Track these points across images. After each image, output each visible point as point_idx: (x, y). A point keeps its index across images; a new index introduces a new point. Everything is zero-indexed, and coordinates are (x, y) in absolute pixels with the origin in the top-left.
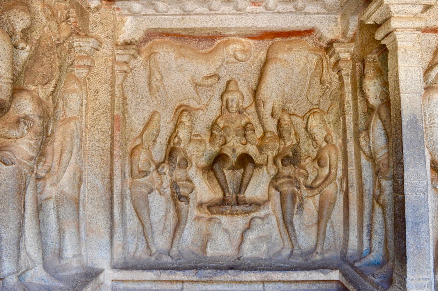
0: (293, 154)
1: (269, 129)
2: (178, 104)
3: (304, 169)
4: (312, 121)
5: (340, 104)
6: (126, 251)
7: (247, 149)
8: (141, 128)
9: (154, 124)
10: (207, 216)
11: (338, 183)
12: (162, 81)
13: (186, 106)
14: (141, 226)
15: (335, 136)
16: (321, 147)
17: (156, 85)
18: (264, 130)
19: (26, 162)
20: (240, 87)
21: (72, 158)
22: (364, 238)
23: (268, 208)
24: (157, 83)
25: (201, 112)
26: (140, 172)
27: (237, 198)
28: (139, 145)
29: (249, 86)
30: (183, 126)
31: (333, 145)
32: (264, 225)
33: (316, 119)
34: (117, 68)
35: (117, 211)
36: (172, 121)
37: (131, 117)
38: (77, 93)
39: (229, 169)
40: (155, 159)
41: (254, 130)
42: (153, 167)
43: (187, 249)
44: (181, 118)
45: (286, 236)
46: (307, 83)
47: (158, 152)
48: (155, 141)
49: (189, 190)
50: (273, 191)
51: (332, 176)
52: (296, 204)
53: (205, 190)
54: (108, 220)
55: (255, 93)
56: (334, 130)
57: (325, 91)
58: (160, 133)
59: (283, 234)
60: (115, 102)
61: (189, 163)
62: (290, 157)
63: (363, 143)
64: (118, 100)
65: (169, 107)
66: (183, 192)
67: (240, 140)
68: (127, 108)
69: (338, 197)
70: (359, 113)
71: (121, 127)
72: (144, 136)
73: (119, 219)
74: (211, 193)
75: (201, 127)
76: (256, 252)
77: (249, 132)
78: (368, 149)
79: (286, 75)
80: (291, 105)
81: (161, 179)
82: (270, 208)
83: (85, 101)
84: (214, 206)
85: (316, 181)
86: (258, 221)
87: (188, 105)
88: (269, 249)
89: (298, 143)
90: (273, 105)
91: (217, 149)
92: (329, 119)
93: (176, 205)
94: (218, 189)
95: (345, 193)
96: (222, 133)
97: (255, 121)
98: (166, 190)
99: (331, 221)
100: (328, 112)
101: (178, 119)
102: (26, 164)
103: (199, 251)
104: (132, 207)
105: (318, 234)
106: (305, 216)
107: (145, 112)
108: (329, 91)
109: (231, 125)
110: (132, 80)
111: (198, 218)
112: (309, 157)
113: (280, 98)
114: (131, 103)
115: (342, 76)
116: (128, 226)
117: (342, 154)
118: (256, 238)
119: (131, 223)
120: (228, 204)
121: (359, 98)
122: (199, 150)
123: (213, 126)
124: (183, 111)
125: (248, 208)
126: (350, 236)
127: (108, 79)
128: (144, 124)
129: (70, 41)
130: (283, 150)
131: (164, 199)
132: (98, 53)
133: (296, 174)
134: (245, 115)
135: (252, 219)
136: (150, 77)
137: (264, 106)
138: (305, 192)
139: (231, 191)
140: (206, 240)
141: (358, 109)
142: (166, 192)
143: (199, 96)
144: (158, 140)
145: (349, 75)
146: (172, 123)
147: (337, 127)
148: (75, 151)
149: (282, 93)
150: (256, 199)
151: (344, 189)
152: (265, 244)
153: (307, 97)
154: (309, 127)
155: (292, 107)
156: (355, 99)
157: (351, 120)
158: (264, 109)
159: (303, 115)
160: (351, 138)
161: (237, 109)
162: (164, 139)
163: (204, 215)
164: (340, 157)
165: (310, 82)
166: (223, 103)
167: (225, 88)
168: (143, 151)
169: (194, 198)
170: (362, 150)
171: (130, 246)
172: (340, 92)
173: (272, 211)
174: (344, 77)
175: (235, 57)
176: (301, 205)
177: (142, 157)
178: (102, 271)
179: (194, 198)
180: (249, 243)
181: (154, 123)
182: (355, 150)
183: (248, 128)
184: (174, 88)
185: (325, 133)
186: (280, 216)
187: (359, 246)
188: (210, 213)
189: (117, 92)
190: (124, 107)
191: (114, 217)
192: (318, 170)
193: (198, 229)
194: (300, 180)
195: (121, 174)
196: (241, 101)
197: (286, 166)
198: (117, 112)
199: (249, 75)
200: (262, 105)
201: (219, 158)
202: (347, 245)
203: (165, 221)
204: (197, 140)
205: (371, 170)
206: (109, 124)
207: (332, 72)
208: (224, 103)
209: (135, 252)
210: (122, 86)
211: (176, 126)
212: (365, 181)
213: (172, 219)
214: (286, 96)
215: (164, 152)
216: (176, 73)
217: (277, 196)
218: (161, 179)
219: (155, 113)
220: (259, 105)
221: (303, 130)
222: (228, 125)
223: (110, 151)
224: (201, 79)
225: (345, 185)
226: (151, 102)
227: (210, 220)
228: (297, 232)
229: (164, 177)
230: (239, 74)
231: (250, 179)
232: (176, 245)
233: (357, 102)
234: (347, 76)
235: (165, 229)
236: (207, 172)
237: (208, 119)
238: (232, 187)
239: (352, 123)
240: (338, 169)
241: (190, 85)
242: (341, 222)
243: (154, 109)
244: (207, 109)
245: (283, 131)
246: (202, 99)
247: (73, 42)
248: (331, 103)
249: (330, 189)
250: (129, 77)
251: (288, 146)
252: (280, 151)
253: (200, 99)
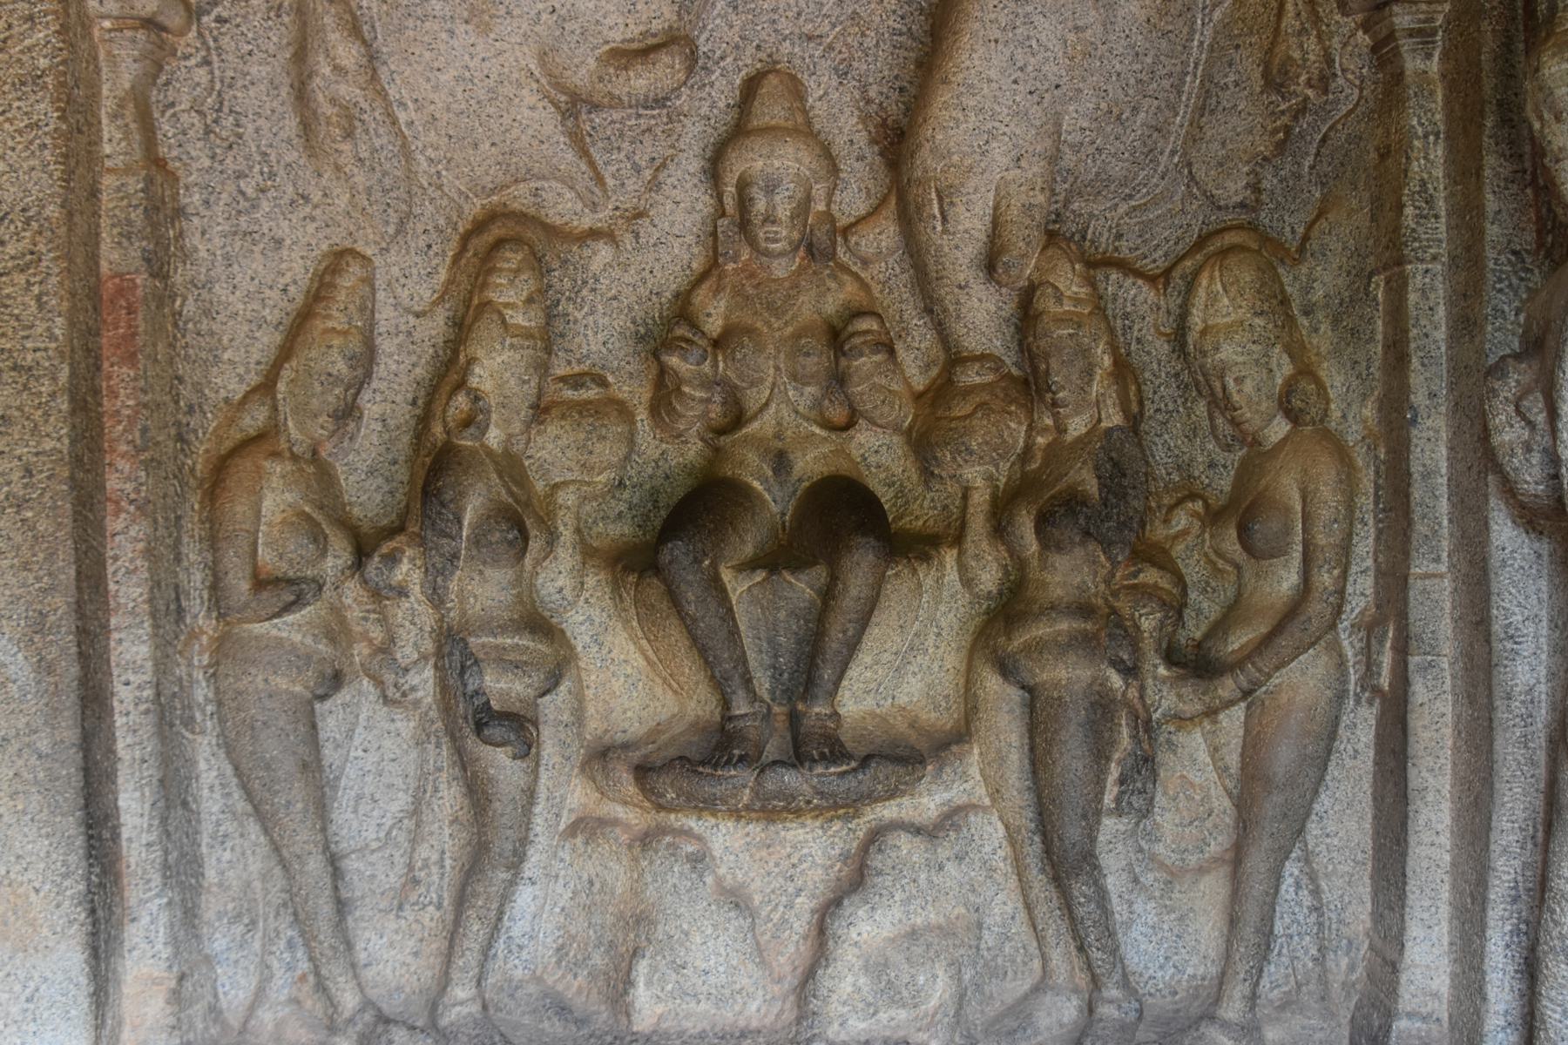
0: (1102, 486)
1: (972, 343)
2: (475, 207)
3: (1161, 568)
4: (1213, 299)
5: (1377, 204)
6: (199, 1009)
7: (856, 454)
8: (269, 339)
9: (338, 321)
10: (632, 815)
11: (1350, 646)
12: (374, 77)
13: (522, 217)
14: (278, 871)
15: (1338, 380)
16: (1256, 442)
17: (333, 101)
18: (947, 349)
20: (819, 110)
22: (1489, 964)
23: (965, 777)
24: (348, 91)
25: (603, 253)
26: (262, 582)
27: (794, 718)
28: (261, 436)
29: (869, 102)
30: (496, 330)
31: (1326, 435)
32: (941, 868)
33: (1233, 289)
35: (133, 805)
36: (441, 299)
37: (209, 284)
39: (750, 566)
40: (356, 511)
41: (892, 352)
42: (337, 558)
43: (532, 988)
44: (485, 285)
45: (1055, 926)
46: (1192, 84)
47: (367, 472)
48: (347, 413)
49: (537, 678)
50: (992, 683)
51: (1317, 608)
52: (1116, 756)
53: (625, 676)
54: (73, 859)
55: (896, 141)
56: (1336, 352)
57: (1287, 130)
58: (380, 371)
59: (1041, 910)
60: (104, 197)
61: (533, 532)
62: (1084, 504)
63: (1508, 433)
64: (119, 190)
65: (420, 228)
66: (501, 693)
67: (817, 404)
68: (181, 234)
69: (1345, 720)
70: (1490, 254)
71: (139, 341)
72: (281, 386)
73: (149, 845)
74: (659, 691)
75: (600, 333)
76: (892, 1012)
77: (865, 363)
78: (1536, 471)
79: (1071, 37)
80: (1097, 208)
81: (383, 621)
82: (974, 771)
84: (668, 765)
85: (1225, 633)
86: (904, 844)
87: (532, 211)
88: (962, 996)
89: (1134, 422)
90: (996, 208)
91: (693, 450)
92: (1307, 290)
94: (689, 669)
95: (1382, 703)
96: (715, 365)
97: (901, 303)
98: (413, 679)
99: (1305, 850)
100: (1302, 249)
101: (471, 292)
103: (594, 996)
104: (229, 770)
105: (1233, 922)
106: (1166, 819)
107: (285, 253)
108: (1315, 127)
109: (770, 327)
110: (201, 75)
111: (586, 827)
112: (1193, 496)
113: (1035, 169)
114: (206, 202)
115: (1391, 36)
116: (211, 875)
117: (1377, 487)
118: (893, 940)
119: (227, 855)
120: (741, 759)
121: (1493, 165)
122: (594, 459)
123: (670, 330)
124: (499, 244)
125: (851, 782)
126: (1408, 945)
127: (43, 63)
128: (287, 321)
130: (1046, 462)
131: (406, 726)
133: (1115, 594)
134: (845, 269)
135: (876, 836)
136: (301, 55)
137: (944, 219)
138: (1165, 693)
139: (763, 683)
140: (629, 939)
141: (1482, 232)
142: (413, 689)
143: (592, 164)
144: (371, 407)
145: (1434, 33)
146: (441, 316)
147: (1354, 332)
149: (1048, 143)
150: (901, 725)
151: (1385, 682)
152: (940, 973)
153: (1190, 165)
154: (1192, 338)
155: (1103, 219)
156: (1465, 171)
157: (1440, 292)
158: (945, 231)
159: (1162, 264)
160: (1432, 395)
161: (796, 235)
162: (399, 399)
163: (620, 811)
164: (1366, 502)
165: (1208, 77)
166: (721, 201)
167: (734, 113)
168: (277, 468)
169: (566, 717)
170: (1498, 469)
171: (222, 979)
172: (1380, 131)
173: (978, 790)
174: (1406, 45)
176: (1145, 766)
179: (566, 717)
180: (859, 963)
181: (336, 317)
182: (1451, 466)
183: (857, 340)
184: (445, 117)
185: (1284, 368)
186: (1025, 820)
187: (1456, 1000)
188: (647, 804)
189: (114, 142)
190: (155, 226)
191: (116, 837)
192: (1238, 567)
193: (591, 883)
194: (1137, 628)
195: (151, 601)
196: (819, 190)
197: (1059, 548)
198: (115, 256)
199: (869, 42)
200: (936, 211)
202: (1393, 991)
203: (414, 842)
204: (583, 407)
205: (1543, 584)
206: (59, 326)
207: (1338, 17)
208: (730, 203)
209: (252, 1009)
211: (461, 329)
212: (1509, 645)
213: (447, 831)
214: (1069, 159)
215: (402, 474)
216: (451, 33)
217: (1011, 711)
218: (385, 619)
219: (339, 259)
220: (919, 209)
221: (1162, 348)
222: (747, 319)
223: (72, 478)
224: (591, 62)
225: (1386, 659)
226: (316, 197)
227: (646, 840)
228: (1117, 906)
229: (399, 612)
230: (810, 38)
231: (864, 621)
232: (464, 970)
233: (1480, 189)
234: (1423, 35)
235: (416, 882)
236: (632, 578)
237: (643, 291)
238: (767, 660)
239: (1441, 311)
240: (1354, 569)
241: (531, 99)
242: (1360, 857)
243: (339, 238)
244: (637, 236)
245: (1047, 356)
246: (610, 182)
248: (1324, 199)
249: (1303, 679)
250: (186, 57)
251: (1079, 440)
252: (1034, 466)
253: (599, 180)
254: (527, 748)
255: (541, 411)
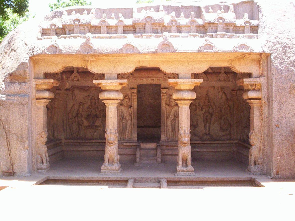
1: (101, 108)
34: (65, 95)
42: (73, 118)
53: (86, 123)
75: (85, 108)
93: (79, 127)
175: (93, 91)
177: (71, 115)
178: (62, 140)
201: (89, 115)
210: (66, 99)
211: (79, 108)
219: (74, 105)
254: (81, 126)
255: (83, 111)
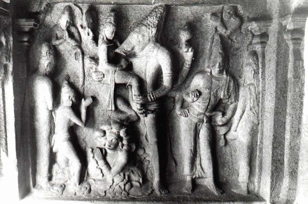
19: (195, 116)
21: (245, 113)
38: (250, 65)
83: (260, 70)
102: (194, 117)
129: (245, 27)
132: (271, 28)
148: (248, 109)
247: (247, 27)
